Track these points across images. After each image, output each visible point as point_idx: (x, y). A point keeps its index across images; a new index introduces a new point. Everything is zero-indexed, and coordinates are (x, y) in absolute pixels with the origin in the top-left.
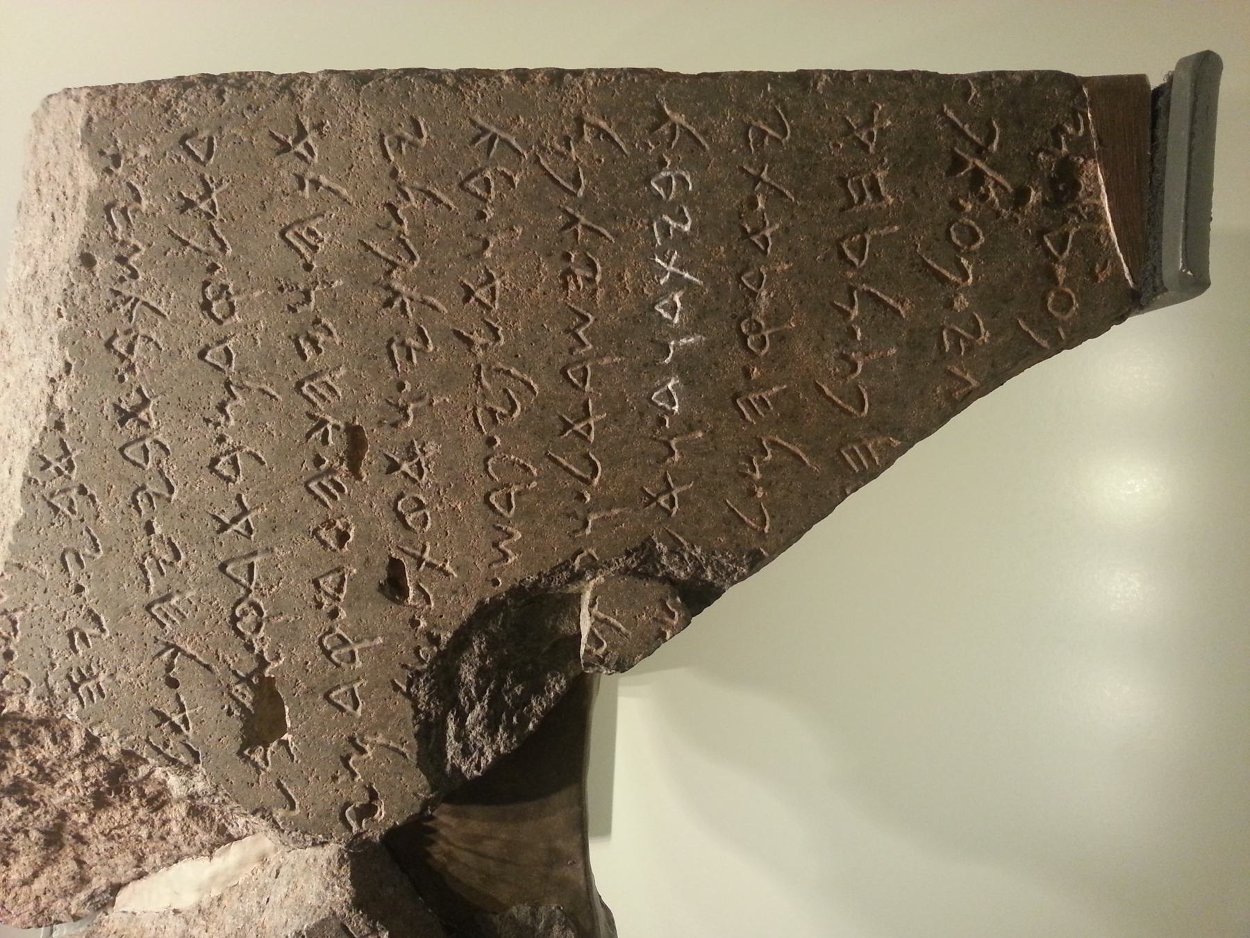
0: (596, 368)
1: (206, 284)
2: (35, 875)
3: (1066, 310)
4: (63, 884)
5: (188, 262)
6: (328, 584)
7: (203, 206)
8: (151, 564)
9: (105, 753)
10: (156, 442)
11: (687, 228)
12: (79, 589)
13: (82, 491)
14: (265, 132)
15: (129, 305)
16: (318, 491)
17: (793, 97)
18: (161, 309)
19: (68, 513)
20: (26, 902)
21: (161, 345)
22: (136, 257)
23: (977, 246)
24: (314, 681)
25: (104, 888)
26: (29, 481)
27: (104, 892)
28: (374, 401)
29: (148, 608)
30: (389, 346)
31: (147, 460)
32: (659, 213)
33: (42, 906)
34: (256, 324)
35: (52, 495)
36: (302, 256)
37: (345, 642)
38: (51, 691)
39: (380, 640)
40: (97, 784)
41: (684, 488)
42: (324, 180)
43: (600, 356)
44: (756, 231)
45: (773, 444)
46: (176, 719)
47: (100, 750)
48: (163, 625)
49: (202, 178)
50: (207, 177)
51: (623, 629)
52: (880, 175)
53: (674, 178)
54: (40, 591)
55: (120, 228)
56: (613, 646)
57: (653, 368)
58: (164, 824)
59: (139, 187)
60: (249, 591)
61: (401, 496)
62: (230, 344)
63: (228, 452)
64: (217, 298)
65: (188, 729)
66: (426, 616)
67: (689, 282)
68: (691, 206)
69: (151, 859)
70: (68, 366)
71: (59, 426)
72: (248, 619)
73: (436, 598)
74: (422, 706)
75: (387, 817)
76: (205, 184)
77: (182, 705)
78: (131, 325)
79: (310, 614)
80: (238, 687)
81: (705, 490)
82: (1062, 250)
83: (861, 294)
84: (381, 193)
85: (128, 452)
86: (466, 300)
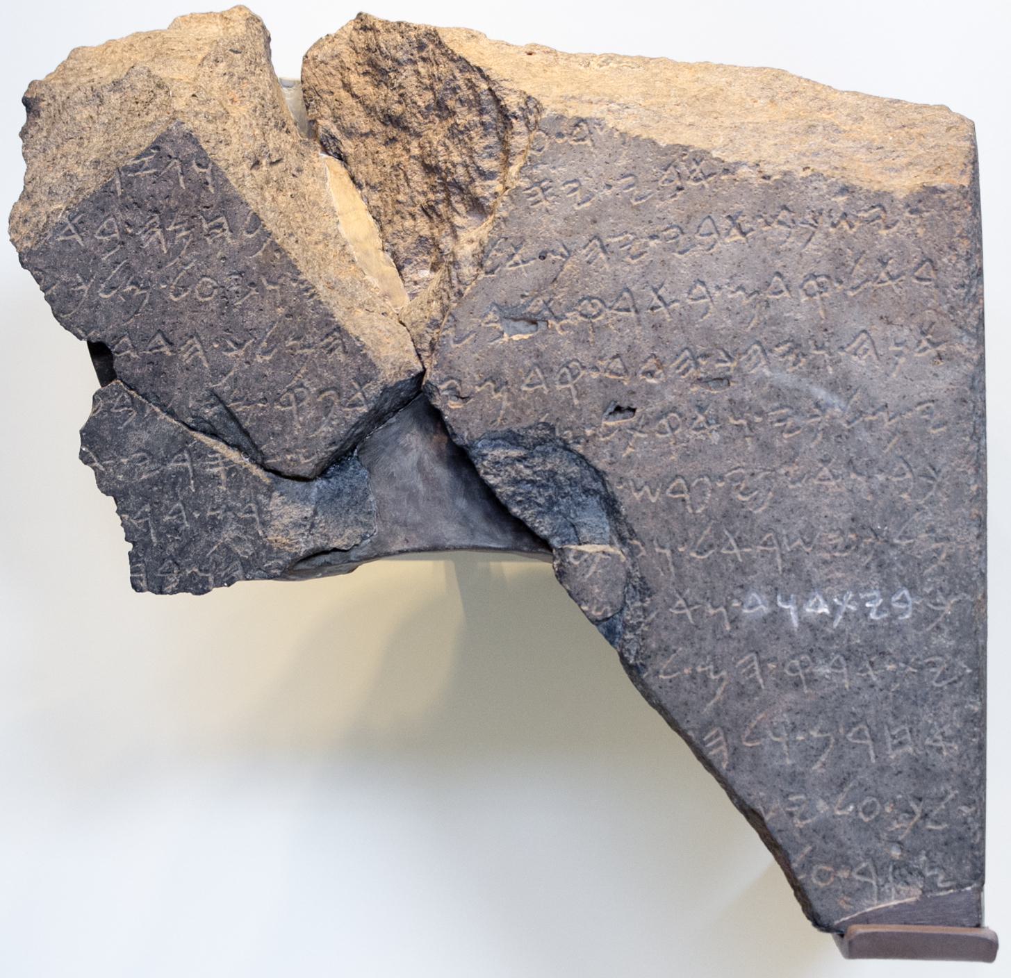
0: (774, 553)
1: (828, 277)
2: (354, 96)
4: (347, 119)
5: (843, 264)
6: (617, 365)
7: (883, 275)
8: (627, 239)
9: (477, 183)
10: (715, 242)
11: (872, 616)
12: (609, 186)
13: (680, 189)
14: (935, 319)
15: (813, 222)
16: (682, 357)
17: (963, 687)
18: (810, 245)
19: (663, 178)
20: (327, 83)
21: (784, 245)
22: (846, 227)
23: (861, 815)
24: (546, 356)
25: (342, 149)
26: (686, 148)
27: (338, 148)
28: (747, 395)
29: (597, 237)
30: (787, 406)
31: (701, 235)
32: (883, 596)
33: (325, 96)
34: (799, 311)
35: (675, 167)
36: (849, 345)
37: (574, 377)
38: (535, 166)
39: (576, 402)
40: (448, 171)
41: (690, 617)
42: (902, 360)
43: (782, 555)
44: (872, 664)
45: (721, 680)
46: (517, 258)
47: (478, 180)
48: (584, 248)
49: (902, 273)
50: (904, 278)
51: (587, 576)
53: (906, 606)
54: (607, 158)
55: (866, 215)
56: (575, 569)
58: (410, 214)
59: (895, 229)
60: (610, 308)
61: (680, 415)
62: (786, 294)
63: (708, 293)
64: (818, 285)
65: (511, 266)
66: (595, 435)
67: (833, 619)
68: (889, 620)
69: (376, 196)
70: (769, 178)
71: (726, 171)
72: (590, 309)
73: (607, 443)
74: (532, 432)
75: (451, 410)
76: (899, 276)
77: (528, 262)
78: (798, 223)
79: (594, 352)
80: (541, 302)
81: (689, 632)
82: (862, 873)
83: (827, 739)
84: (892, 398)
85: (708, 221)
86: (822, 461)
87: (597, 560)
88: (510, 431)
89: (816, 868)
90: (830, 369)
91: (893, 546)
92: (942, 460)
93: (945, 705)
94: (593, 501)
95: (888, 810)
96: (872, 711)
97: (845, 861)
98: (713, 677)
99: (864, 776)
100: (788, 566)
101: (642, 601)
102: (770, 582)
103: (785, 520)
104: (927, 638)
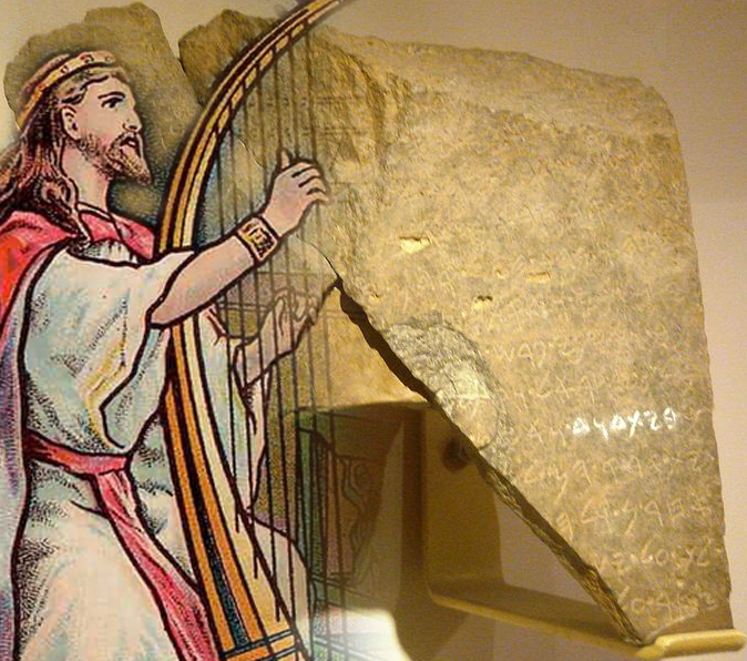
3: (636, 607)
42: (653, 254)
43: (595, 394)
44: (654, 460)
52: (682, 514)
57: (591, 416)
82: (662, 601)
87: (477, 404)
88: (413, 318)
89: (633, 602)
90: (612, 263)
91: (661, 380)
92: (685, 319)
93: (701, 483)
94: (466, 364)
95: (673, 555)
96: (658, 492)
97: (650, 594)
98: (558, 478)
99: (657, 535)
100: (598, 398)
101: (508, 430)
102: (589, 411)
103: (593, 367)
104: (686, 438)
